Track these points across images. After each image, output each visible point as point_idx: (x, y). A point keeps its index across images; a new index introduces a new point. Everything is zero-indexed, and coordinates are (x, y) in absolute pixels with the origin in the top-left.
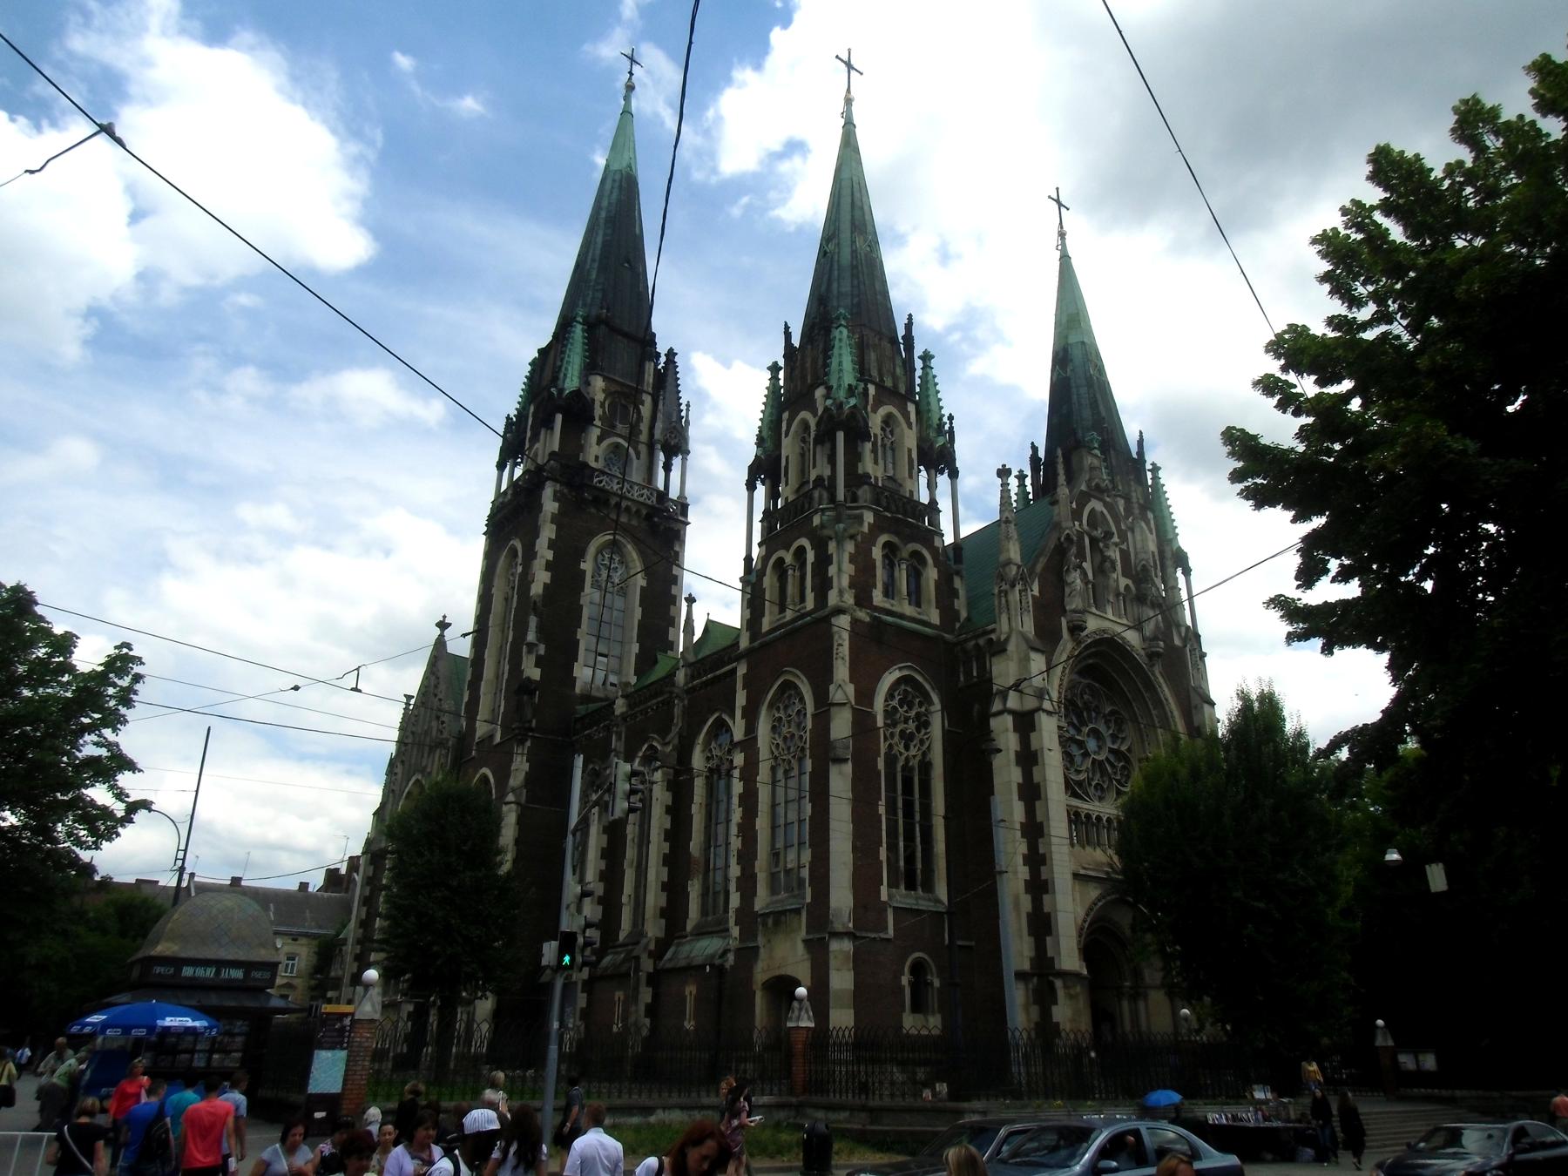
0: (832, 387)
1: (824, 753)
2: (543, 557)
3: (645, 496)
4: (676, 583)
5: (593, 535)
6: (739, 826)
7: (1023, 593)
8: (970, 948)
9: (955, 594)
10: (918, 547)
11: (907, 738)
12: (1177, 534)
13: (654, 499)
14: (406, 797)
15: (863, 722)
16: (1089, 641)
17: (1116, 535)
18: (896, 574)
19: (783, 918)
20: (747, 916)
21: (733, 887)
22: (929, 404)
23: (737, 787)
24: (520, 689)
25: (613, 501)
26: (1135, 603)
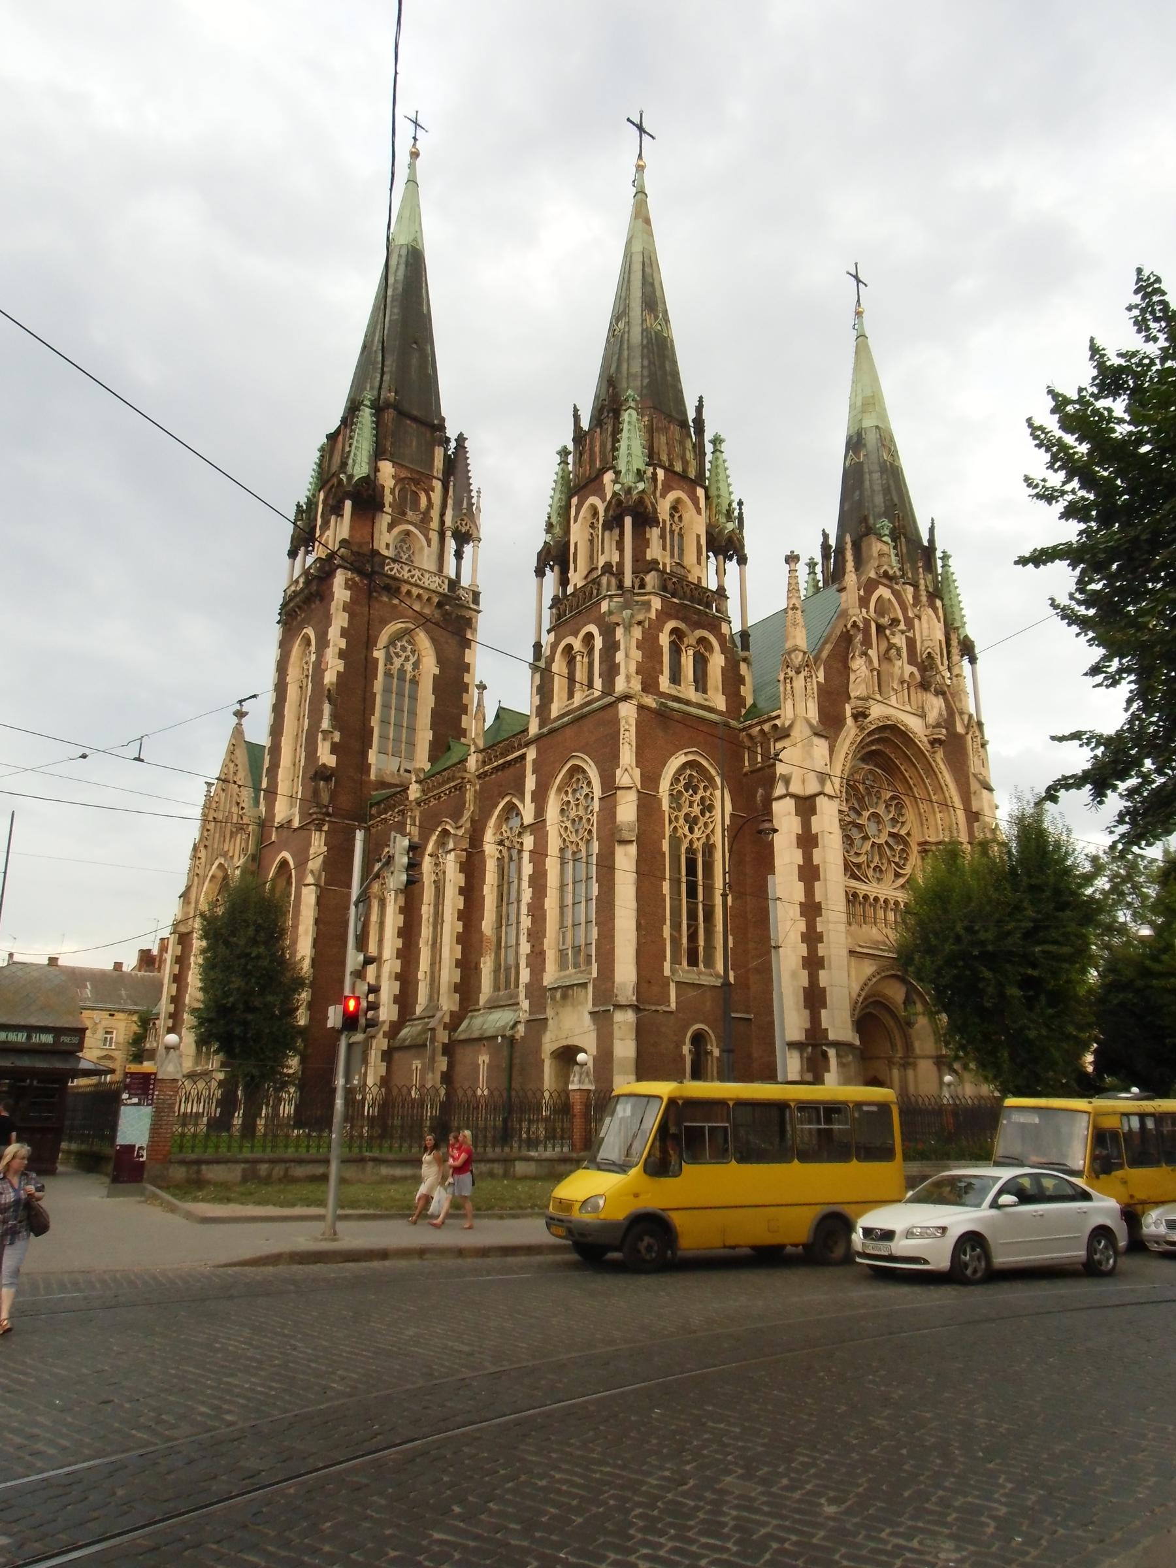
0: (620, 472)
1: (611, 837)
4: (468, 672)
5: (384, 622)
6: (528, 904)
7: (808, 680)
8: (750, 1020)
9: (741, 680)
10: (705, 633)
11: (692, 822)
12: (965, 623)
13: (446, 587)
14: (211, 880)
15: (647, 804)
16: (873, 727)
17: (902, 623)
18: (683, 660)
19: (570, 992)
20: (537, 992)
21: (523, 962)
22: (718, 489)
23: (527, 869)
24: (320, 774)
25: (405, 588)
26: (919, 690)
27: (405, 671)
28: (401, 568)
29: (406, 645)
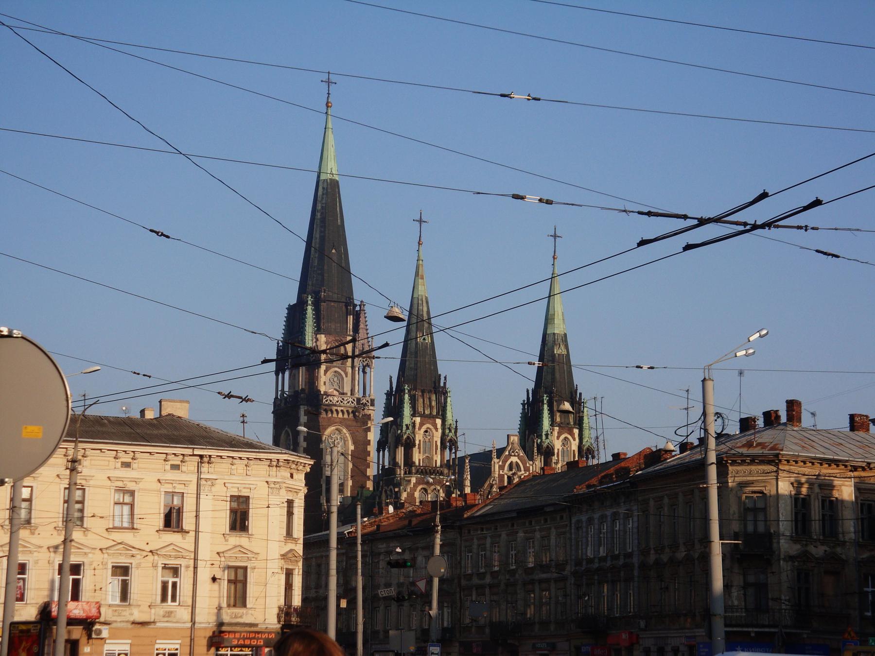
2: (302, 446)
3: (350, 402)
13: (355, 403)
25: (334, 408)
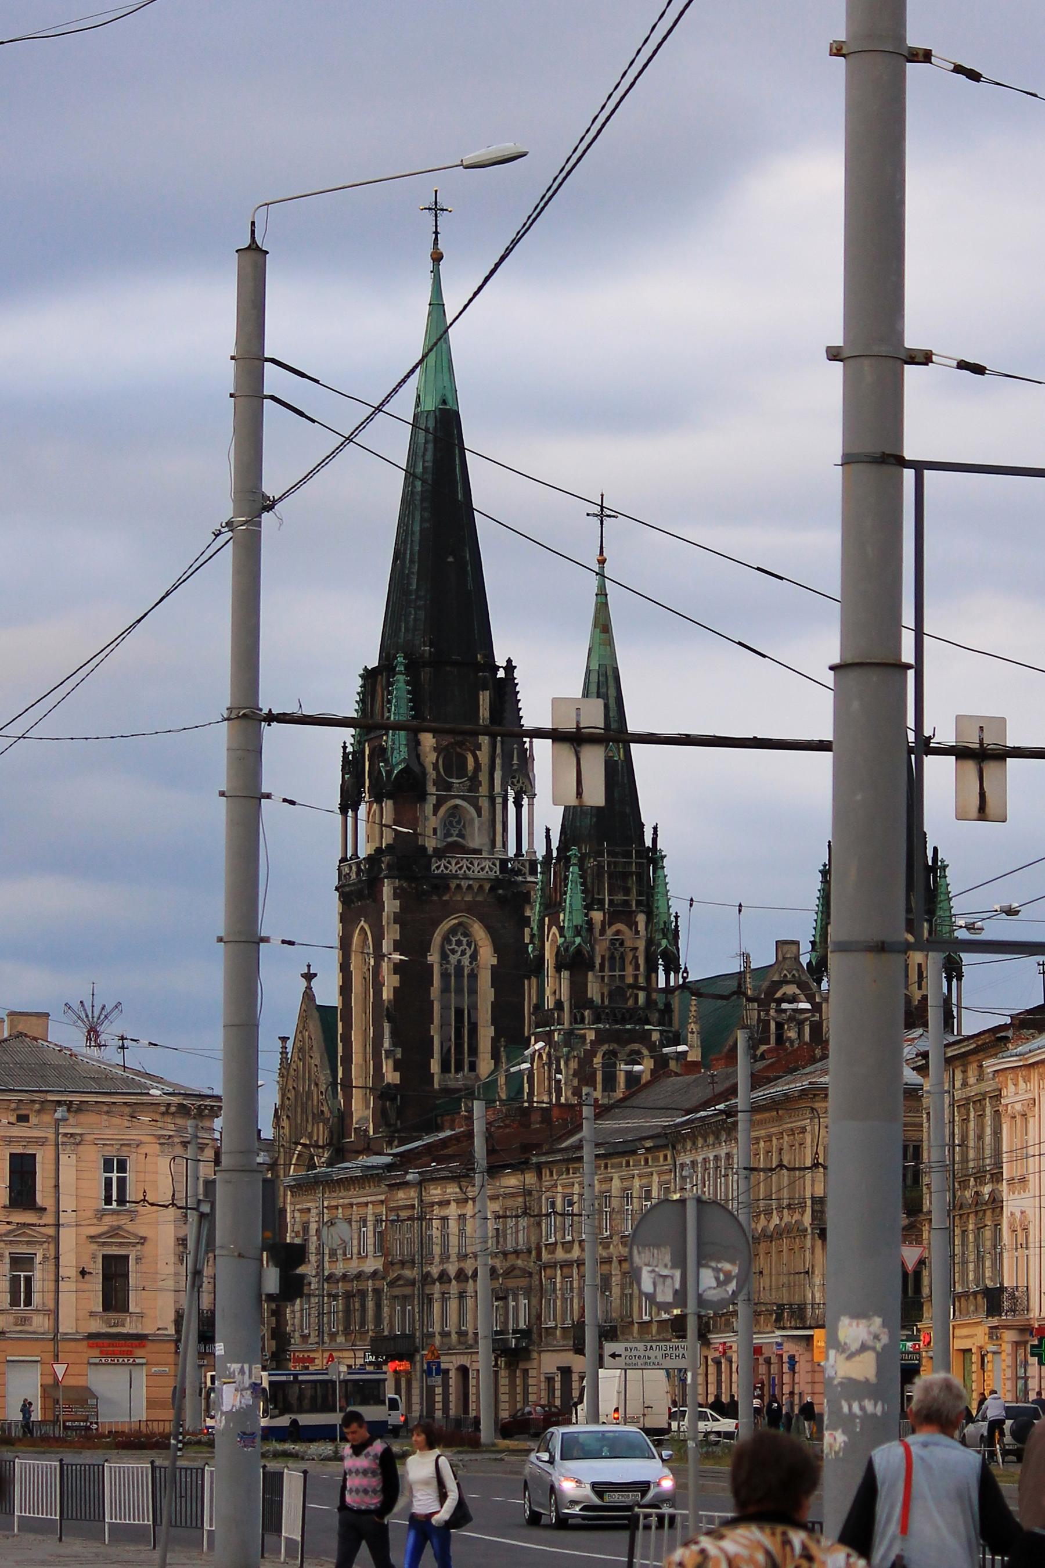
3: (487, 869)
13: (497, 869)
25: (453, 886)
27: (463, 967)
28: (449, 863)
29: (462, 939)
